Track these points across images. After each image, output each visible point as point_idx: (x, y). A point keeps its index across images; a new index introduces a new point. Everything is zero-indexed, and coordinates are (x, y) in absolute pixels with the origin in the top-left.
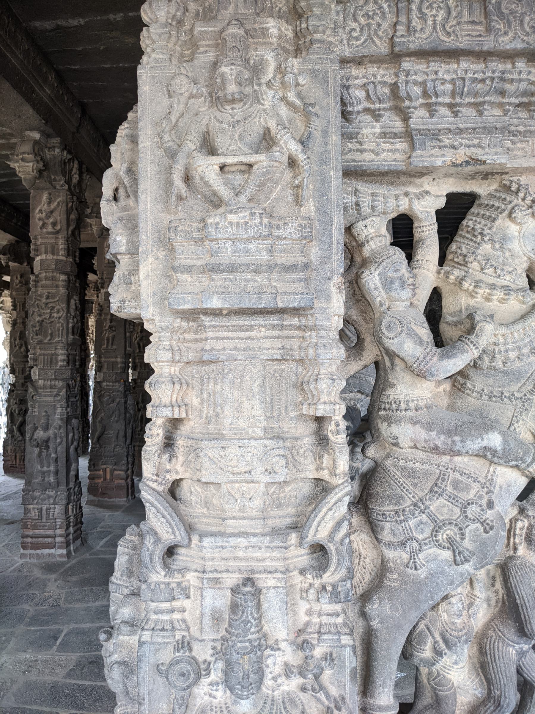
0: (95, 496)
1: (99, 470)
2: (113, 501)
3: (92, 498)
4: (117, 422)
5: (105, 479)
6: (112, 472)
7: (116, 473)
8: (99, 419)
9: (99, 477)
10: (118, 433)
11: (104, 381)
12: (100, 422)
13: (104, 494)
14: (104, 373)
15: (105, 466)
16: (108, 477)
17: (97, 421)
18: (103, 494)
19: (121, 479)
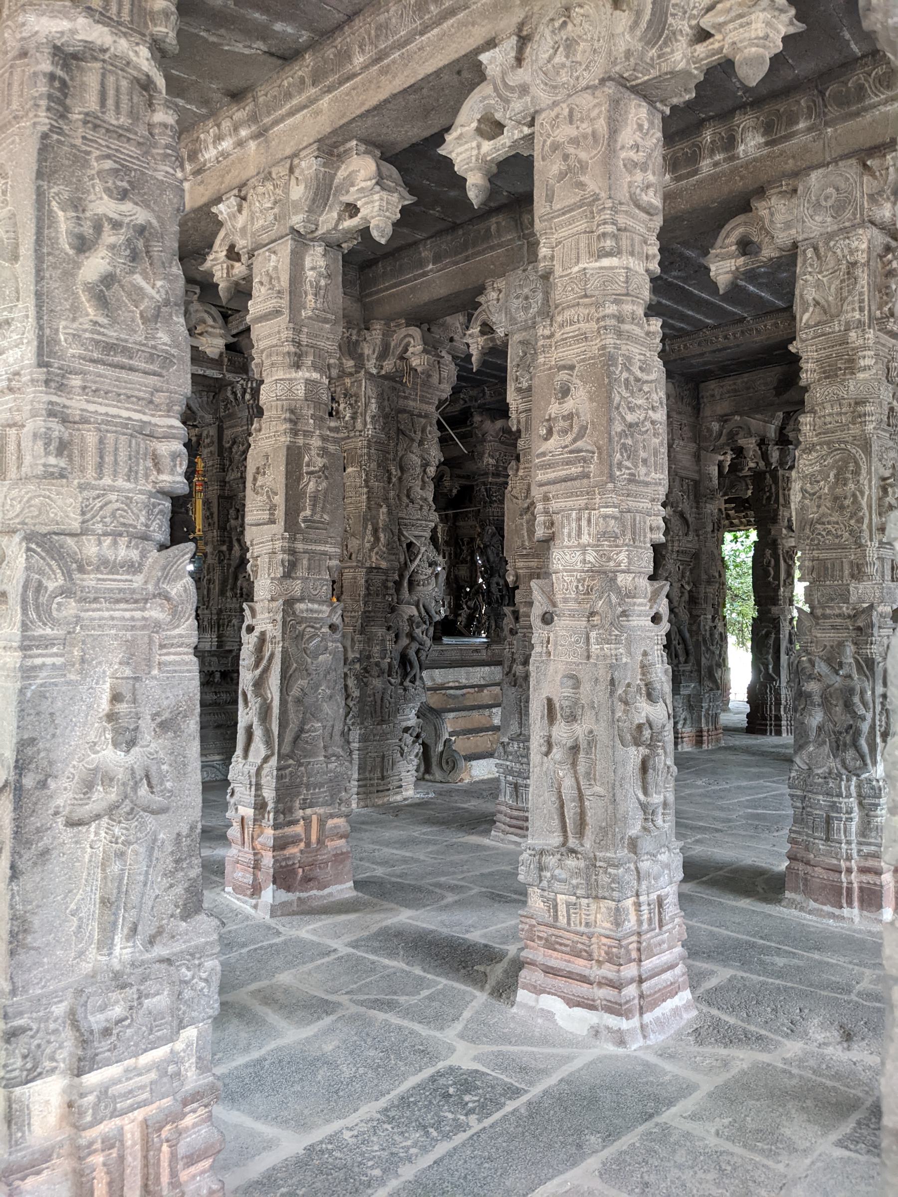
0: (288, 889)
1: (294, 822)
2: (330, 894)
3: (284, 896)
4: (331, 697)
5: (308, 844)
6: (322, 822)
7: (331, 823)
8: (295, 692)
9: (295, 840)
10: (333, 726)
11: (301, 600)
12: (299, 701)
13: (310, 880)
14: (305, 579)
15: (309, 811)
16: (314, 838)
17: (290, 699)
18: (308, 880)
19: (341, 837)
